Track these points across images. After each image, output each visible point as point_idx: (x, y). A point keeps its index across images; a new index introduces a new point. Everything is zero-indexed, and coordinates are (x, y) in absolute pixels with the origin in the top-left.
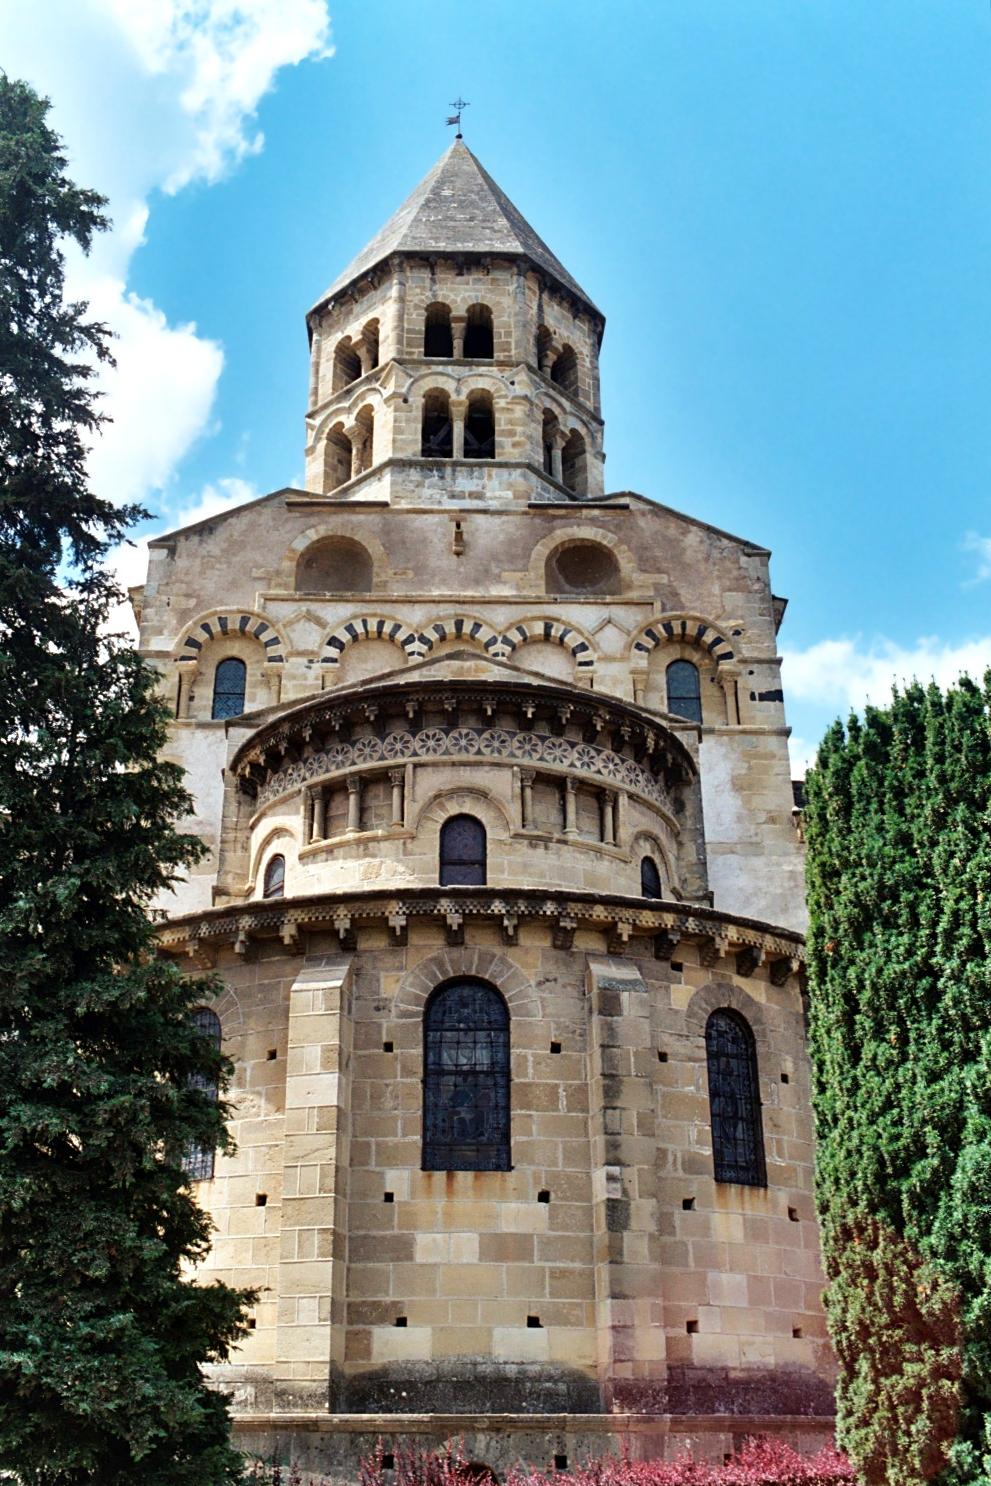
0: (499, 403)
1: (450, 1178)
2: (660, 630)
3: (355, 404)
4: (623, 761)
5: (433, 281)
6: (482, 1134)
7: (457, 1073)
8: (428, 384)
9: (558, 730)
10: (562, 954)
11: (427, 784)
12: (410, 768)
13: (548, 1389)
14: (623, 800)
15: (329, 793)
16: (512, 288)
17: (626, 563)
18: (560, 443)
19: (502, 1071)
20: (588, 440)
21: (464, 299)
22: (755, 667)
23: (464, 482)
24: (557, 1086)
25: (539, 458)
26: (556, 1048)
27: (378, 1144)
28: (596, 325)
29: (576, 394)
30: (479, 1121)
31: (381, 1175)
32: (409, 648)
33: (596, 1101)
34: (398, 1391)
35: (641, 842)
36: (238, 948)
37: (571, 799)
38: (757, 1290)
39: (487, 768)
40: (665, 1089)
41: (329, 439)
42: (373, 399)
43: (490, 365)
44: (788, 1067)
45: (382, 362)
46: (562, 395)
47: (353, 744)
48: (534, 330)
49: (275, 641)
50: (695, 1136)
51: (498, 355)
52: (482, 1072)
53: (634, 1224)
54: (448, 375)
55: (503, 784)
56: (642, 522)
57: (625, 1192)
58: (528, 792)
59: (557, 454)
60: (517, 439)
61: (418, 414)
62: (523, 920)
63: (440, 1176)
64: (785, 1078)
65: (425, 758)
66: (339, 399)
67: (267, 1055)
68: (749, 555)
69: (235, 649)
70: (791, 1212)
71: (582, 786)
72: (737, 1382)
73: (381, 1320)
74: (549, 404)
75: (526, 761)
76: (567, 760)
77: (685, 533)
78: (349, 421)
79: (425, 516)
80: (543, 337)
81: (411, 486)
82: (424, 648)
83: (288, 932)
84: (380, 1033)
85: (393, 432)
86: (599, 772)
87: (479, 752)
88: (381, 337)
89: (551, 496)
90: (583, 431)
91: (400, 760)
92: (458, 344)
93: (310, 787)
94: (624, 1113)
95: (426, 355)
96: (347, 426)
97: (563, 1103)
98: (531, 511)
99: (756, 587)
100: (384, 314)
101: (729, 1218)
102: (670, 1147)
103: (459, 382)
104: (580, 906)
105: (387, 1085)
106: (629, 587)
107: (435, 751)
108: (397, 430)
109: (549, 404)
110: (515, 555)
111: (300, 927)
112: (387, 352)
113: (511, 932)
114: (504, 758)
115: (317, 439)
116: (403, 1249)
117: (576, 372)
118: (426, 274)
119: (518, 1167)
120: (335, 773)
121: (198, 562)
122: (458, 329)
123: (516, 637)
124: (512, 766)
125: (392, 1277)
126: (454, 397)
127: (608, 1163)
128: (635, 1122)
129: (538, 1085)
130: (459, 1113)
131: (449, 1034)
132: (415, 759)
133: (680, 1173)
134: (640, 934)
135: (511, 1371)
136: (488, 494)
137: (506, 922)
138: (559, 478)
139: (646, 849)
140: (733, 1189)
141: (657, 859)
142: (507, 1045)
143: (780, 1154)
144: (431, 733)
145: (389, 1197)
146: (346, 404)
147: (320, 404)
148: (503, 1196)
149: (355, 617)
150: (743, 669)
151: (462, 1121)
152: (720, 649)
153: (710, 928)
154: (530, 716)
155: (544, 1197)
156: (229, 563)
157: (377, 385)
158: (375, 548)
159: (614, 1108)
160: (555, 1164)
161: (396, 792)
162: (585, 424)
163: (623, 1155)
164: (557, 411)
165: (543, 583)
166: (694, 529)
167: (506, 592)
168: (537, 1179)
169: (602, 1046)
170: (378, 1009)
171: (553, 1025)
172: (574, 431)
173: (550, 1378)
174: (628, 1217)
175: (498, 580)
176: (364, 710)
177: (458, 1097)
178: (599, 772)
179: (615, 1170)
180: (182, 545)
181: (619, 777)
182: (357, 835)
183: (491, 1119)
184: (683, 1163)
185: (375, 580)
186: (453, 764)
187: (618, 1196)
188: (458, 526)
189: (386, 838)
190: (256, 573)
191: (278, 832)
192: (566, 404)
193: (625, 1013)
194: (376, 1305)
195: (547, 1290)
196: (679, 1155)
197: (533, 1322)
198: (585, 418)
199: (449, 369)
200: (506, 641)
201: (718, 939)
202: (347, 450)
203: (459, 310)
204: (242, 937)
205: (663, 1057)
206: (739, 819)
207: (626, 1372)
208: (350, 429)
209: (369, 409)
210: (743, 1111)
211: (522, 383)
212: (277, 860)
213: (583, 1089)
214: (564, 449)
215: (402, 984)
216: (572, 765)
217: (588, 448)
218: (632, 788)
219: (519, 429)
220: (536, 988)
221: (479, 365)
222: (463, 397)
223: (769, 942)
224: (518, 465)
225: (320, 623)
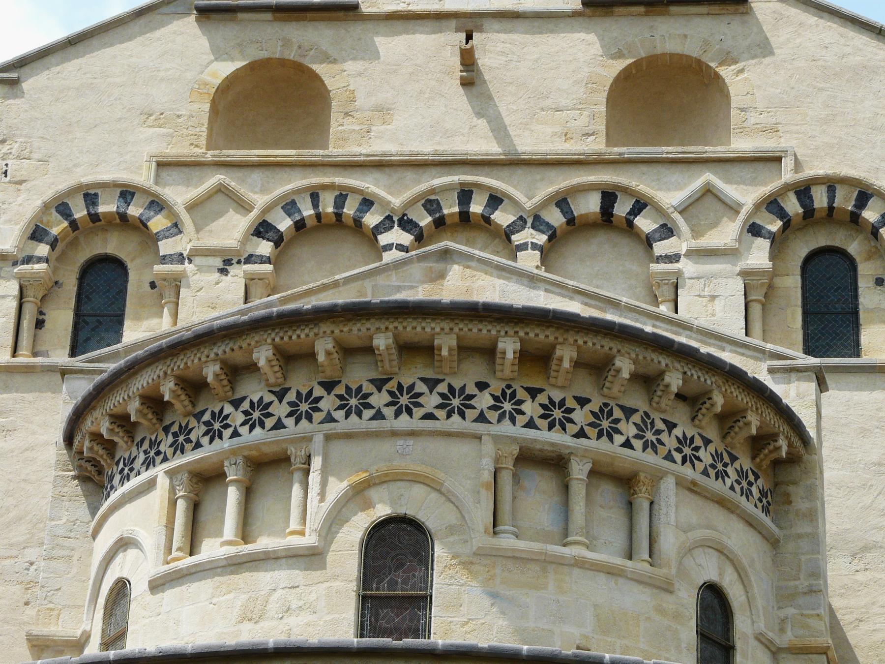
2: (793, 206)
12: (319, 439)
32: (384, 239)
37: (578, 490)
58: (506, 478)
69: (112, 245)
71: (599, 473)
82: (406, 238)
98: (588, 11)
123: (556, 218)
139: (709, 569)
178: (627, 444)
182: (231, 550)
185: (335, 128)
188: (469, 37)
191: (123, 544)
212: (121, 588)
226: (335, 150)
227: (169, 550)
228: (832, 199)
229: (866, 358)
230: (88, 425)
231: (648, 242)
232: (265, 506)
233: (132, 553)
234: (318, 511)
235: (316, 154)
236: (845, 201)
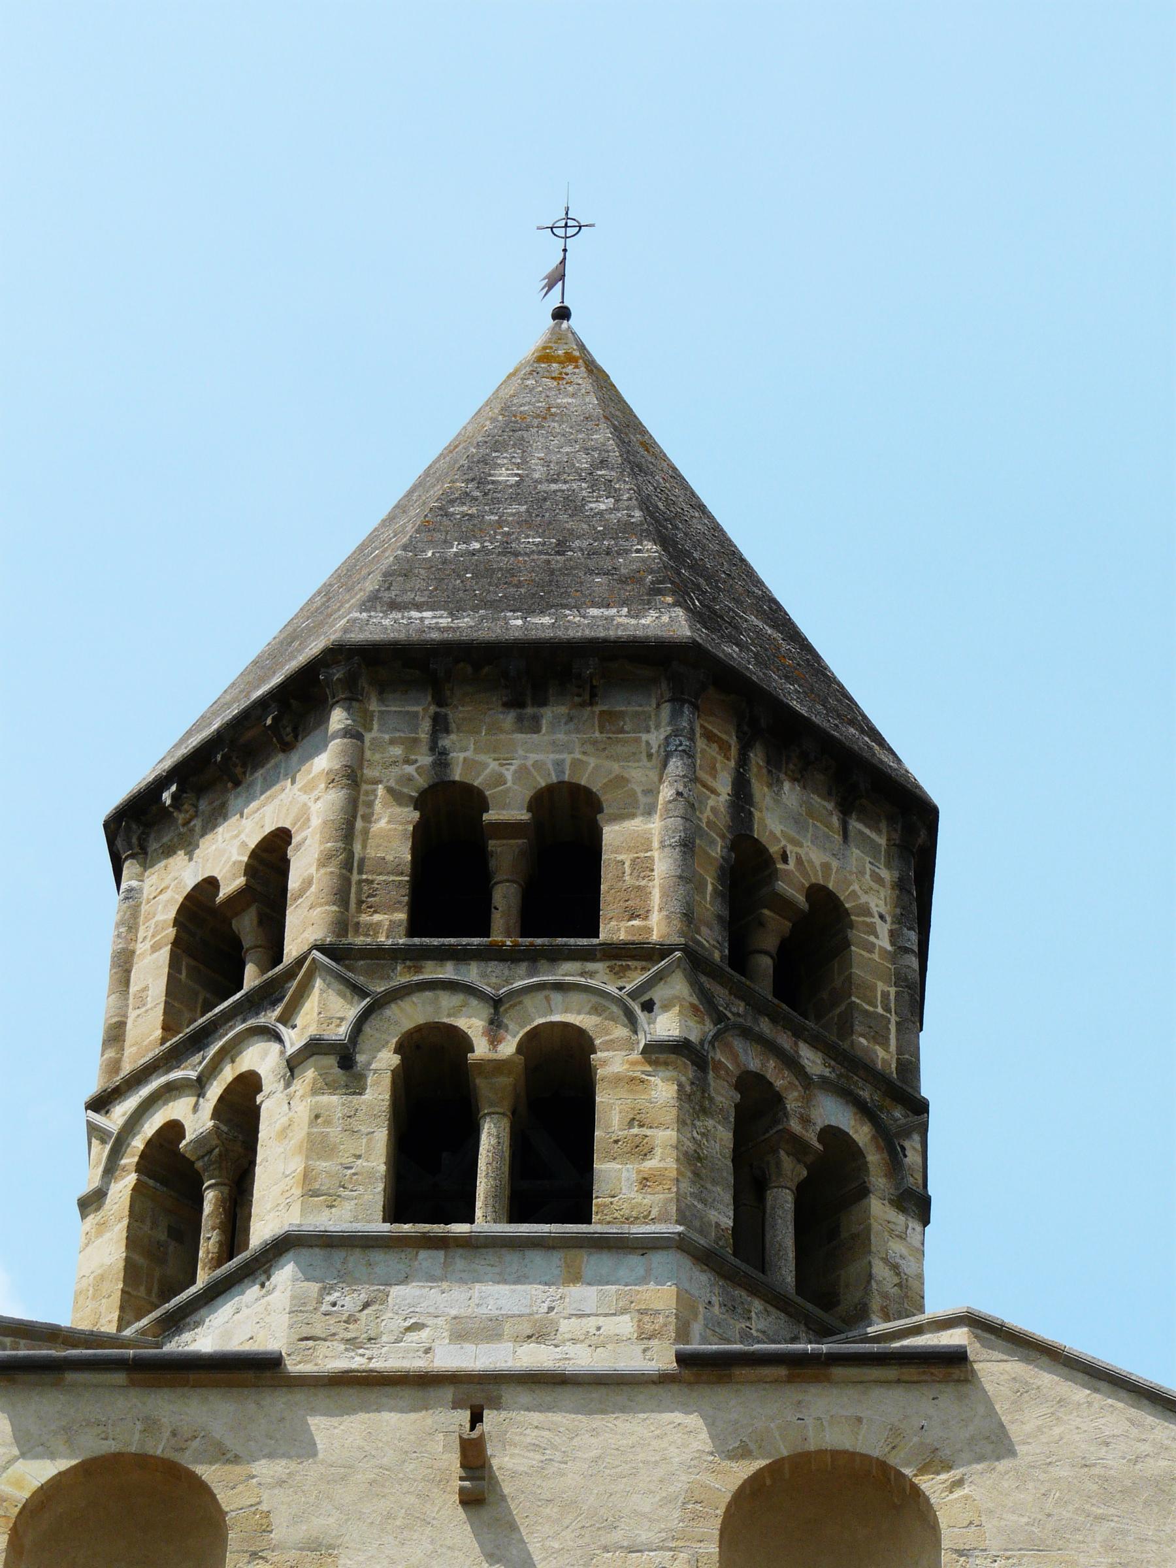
5: (440, 726)
8: (410, 1015)
16: (654, 738)
18: (791, 1170)
20: (874, 1158)
21: (522, 772)
28: (909, 831)
29: (845, 1027)
41: (139, 1168)
42: (261, 1059)
43: (587, 955)
45: (292, 948)
46: (798, 1034)
48: (718, 850)
54: (470, 990)
59: (782, 1203)
61: (378, 1093)
78: (195, 1118)
80: (742, 873)
85: (317, 1153)
88: (293, 883)
89: (761, 1330)
90: (862, 1134)
92: (504, 898)
95: (412, 931)
96: (190, 1136)
98: (686, 1373)
100: (304, 817)
108: (318, 1146)
112: (305, 926)
115: (111, 1170)
117: (847, 963)
118: (422, 708)
126: (481, 1049)
136: (565, 1326)
138: (786, 1273)
146: (187, 1071)
147: (127, 1068)
157: (269, 1017)
162: (865, 1111)
164: (780, 1079)
172: (831, 1135)
192: (812, 1060)
198: (865, 1094)
199: (472, 974)
202: (184, 1204)
203: (509, 807)
208: (200, 1141)
209: (249, 1084)
214: (802, 1193)
217: (878, 1181)
221: (555, 956)
222: (508, 1048)
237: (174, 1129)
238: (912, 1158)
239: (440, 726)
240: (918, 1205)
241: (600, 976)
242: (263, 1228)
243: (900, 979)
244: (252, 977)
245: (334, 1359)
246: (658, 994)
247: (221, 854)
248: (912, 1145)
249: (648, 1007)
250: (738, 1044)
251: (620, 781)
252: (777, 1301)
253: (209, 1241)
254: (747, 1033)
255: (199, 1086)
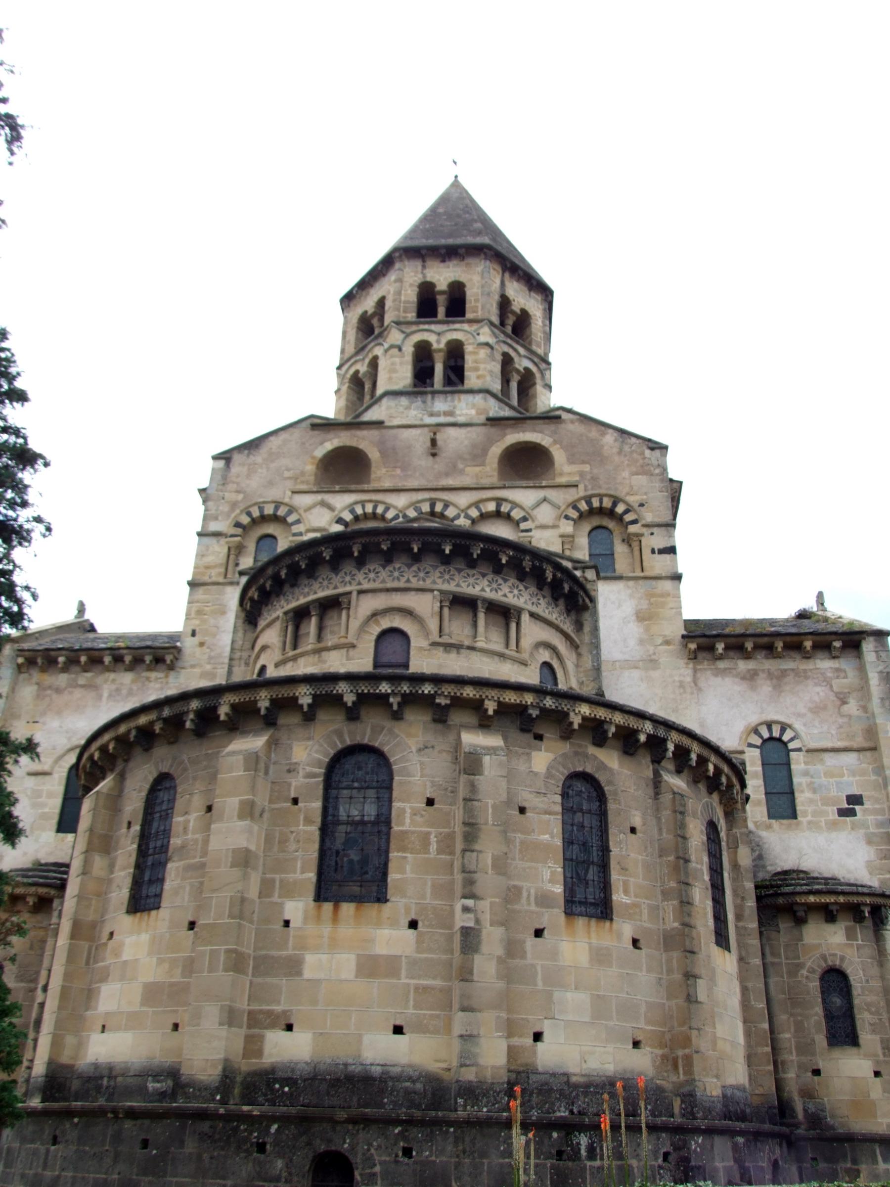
0: (468, 348)
1: (336, 908)
2: (583, 506)
3: (367, 355)
4: (526, 588)
5: (424, 267)
6: (366, 873)
7: (347, 823)
8: (417, 338)
9: (472, 564)
10: (440, 726)
11: (366, 606)
12: (354, 594)
13: (406, 1088)
14: (525, 618)
15: (300, 615)
16: (479, 269)
17: (559, 455)
19: (384, 822)
20: (538, 375)
21: (445, 279)
22: (655, 530)
23: (440, 405)
24: (429, 833)
25: (497, 387)
26: (430, 802)
27: (281, 881)
28: (547, 296)
29: (530, 343)
30: (364, 861)
31: (281, 906)
33: (459, 845)
34: (282, 1087)
35: (541, 650)
36: (188, 725)
37: (481, 616)
38: (600, 1006)
39: (413, 593)
40: (523, 836)
42: (378, 351)
43: (462, 322)
44: (637, 821)
45: (386, 324)
46: (518, 343)
47: (316, 579)
48: (497, 297)
49: (298, 522)
50: (549, 877)
51: (469, 315)
52: (370, 822)
53: (485, 948)
55: (425, 605)
56: (571, 427)
57: (477, 921)
59: (514, 385)
60: (480, 373)
62: (408, 700)
63: (328, 907)
64: (633, 830)
65: (366, 586)
66: (357, 353)
67: (204, 809)
68: (652, 449)
70: (635, 943)
72: (576, 1086)
73: (272, 1026)
74: (506, 349)
75: (445, 587)
76: (479, 586)
77: (603, 434)
78: (363, 368)
79: (410, 430)
80: (504, 303)
81: (401, 409)
83: (223, 711)
84: (289, 790)
86: (505, 596)
87: (408, 581)
88: (386, 308)
90: (534, 369)
91: (348, 588)
92: (441, 311)
93: (286, 613)
94: (480, 856)
96: (361, 372)
97: (434, 847)
98: (488, 423)
99: (657, 471)
100: (389, 292)
101: (574, 944)
102: (525, 885)
103: (438, 336)
104: (453, 686)
105: (292, 832)
106: (561, 474)
107: (374, 581)
109: (506, 349)
110: (478, 455)
111: (234, 707)
112: (388, 319)
113: (395, 707)
114: (428, 584)
116: (294, 966)
117: (530, 329)
118: (418, 263)
119: (393, 899)
120: (302, 601)
121: (246, 468)
122: (442, 301)
124: (432, 591)
125: (284, 989)
126: (435, 346)
127: (465, 897)
128: (489, 862)
129: (413, 832)
130: (347, 855)
131: (345, 792)
132: (359, 587)
133: (533, 907)
134: (503, 709)
135: (376, 1070)
136: (458, 412)
137: (391, 700)
138: (515, 402)
139: (545, 655)
140: (581, 922)
141: (555, 664)
142: (390, 801)
143: (626, 892)
144: (372, 568)
145: (287, 923)
147: (345, 358)
148: (379, 924)
149: (356, 503)
150: (645, 531)
151: (351, 861)
152: (628, 518)
153: (565, 706)
154: (447, 552)
155: (413, 925)
156: (268, 469)
157: (380, 340)
158: (374, 454)
159: (473, 851)
160: (423, 897)
161: (344, 613)
163: (478, 889)
164: (513, 354)
165: (496, 474)
166: (610, 431)
167: (467, 481)
168: (408, 909)
169: (464, 799)
170: (289, 771)
171: (429, 784)
172: (527, 369)
173: (410, 1079)
174: (479, 943)
175: (462, 472)
176: (322, 553)
177: (349, 842)
178: (505, 596)
179: (470, 903)
180: (237, 457)
181: (522, 600)
183: (376, 861)
184: (536, 898)
185: (373, 476)
186: (388, 590)
187: (471, 924)
189: (336, 647)
190: (287, 474)
192: (522, 351)
193: (486, 773)
194: (269, 1013)
195: (411, 1003)
196: (533, 892)
197: (398, 1030)
198: (536, 360)
200: (467, 516)
201: (572, 714)
202: (359, 387)
204: (191, 716)
205: (522, 810)
206: (641, 642)
207: (469, 1075)
210: (595, 855)
211: (486, 335)
213: (451, 836)
214: (520, 384)
215: (308, 752)
216: (483, 590)
218: (534, 609)
219: (482, 366)
220: (417, 757)
221: (454, 322)
222: (442, 346)
223: (618, 718)
224: (480, 391)
225: (331, 508)
226: (374, 485)
227: (284, 649)
228: (601, 502)
229: (618, 573)
230: (250, 594)
231: (517, 523)
232: (329, 623)
233: (269, 651)
234: (355, 624)
235: (366, 487)
236: (607, 503)
237: (357, 372)
238: (547, 376)
239: (424, 267)
240: (549, 387)
241: (466, 326)
242: (379, 391)
243: (544, 332)
244: (377, 332)
245: (396, 422)
246: (481, 331)
247: (368, 304)
248: (547, 372)
249: (478, 334)
250: (502, 345)
251: (471, 280)
252: (511, 407)
253: (367, 397)
254: (505, 342)
255: (363, 359)
